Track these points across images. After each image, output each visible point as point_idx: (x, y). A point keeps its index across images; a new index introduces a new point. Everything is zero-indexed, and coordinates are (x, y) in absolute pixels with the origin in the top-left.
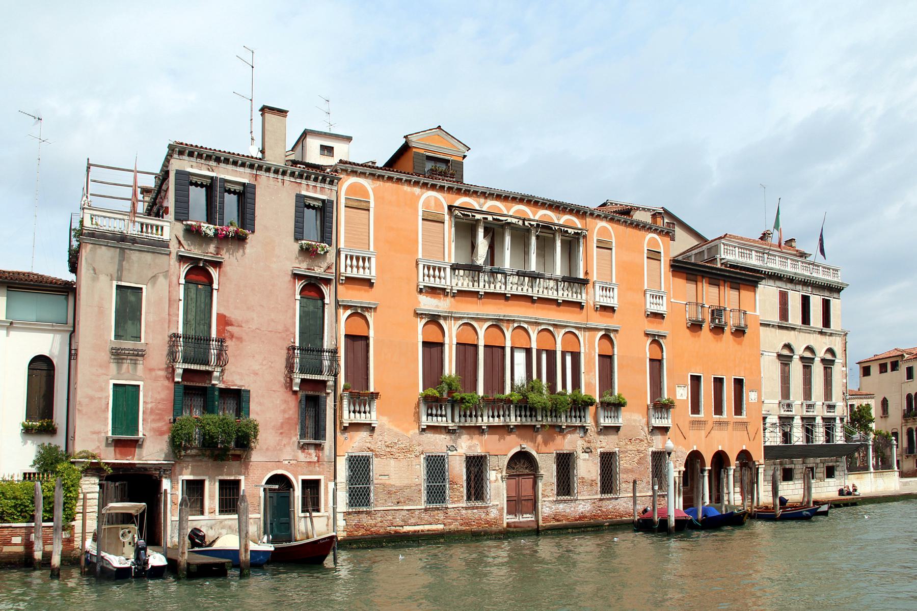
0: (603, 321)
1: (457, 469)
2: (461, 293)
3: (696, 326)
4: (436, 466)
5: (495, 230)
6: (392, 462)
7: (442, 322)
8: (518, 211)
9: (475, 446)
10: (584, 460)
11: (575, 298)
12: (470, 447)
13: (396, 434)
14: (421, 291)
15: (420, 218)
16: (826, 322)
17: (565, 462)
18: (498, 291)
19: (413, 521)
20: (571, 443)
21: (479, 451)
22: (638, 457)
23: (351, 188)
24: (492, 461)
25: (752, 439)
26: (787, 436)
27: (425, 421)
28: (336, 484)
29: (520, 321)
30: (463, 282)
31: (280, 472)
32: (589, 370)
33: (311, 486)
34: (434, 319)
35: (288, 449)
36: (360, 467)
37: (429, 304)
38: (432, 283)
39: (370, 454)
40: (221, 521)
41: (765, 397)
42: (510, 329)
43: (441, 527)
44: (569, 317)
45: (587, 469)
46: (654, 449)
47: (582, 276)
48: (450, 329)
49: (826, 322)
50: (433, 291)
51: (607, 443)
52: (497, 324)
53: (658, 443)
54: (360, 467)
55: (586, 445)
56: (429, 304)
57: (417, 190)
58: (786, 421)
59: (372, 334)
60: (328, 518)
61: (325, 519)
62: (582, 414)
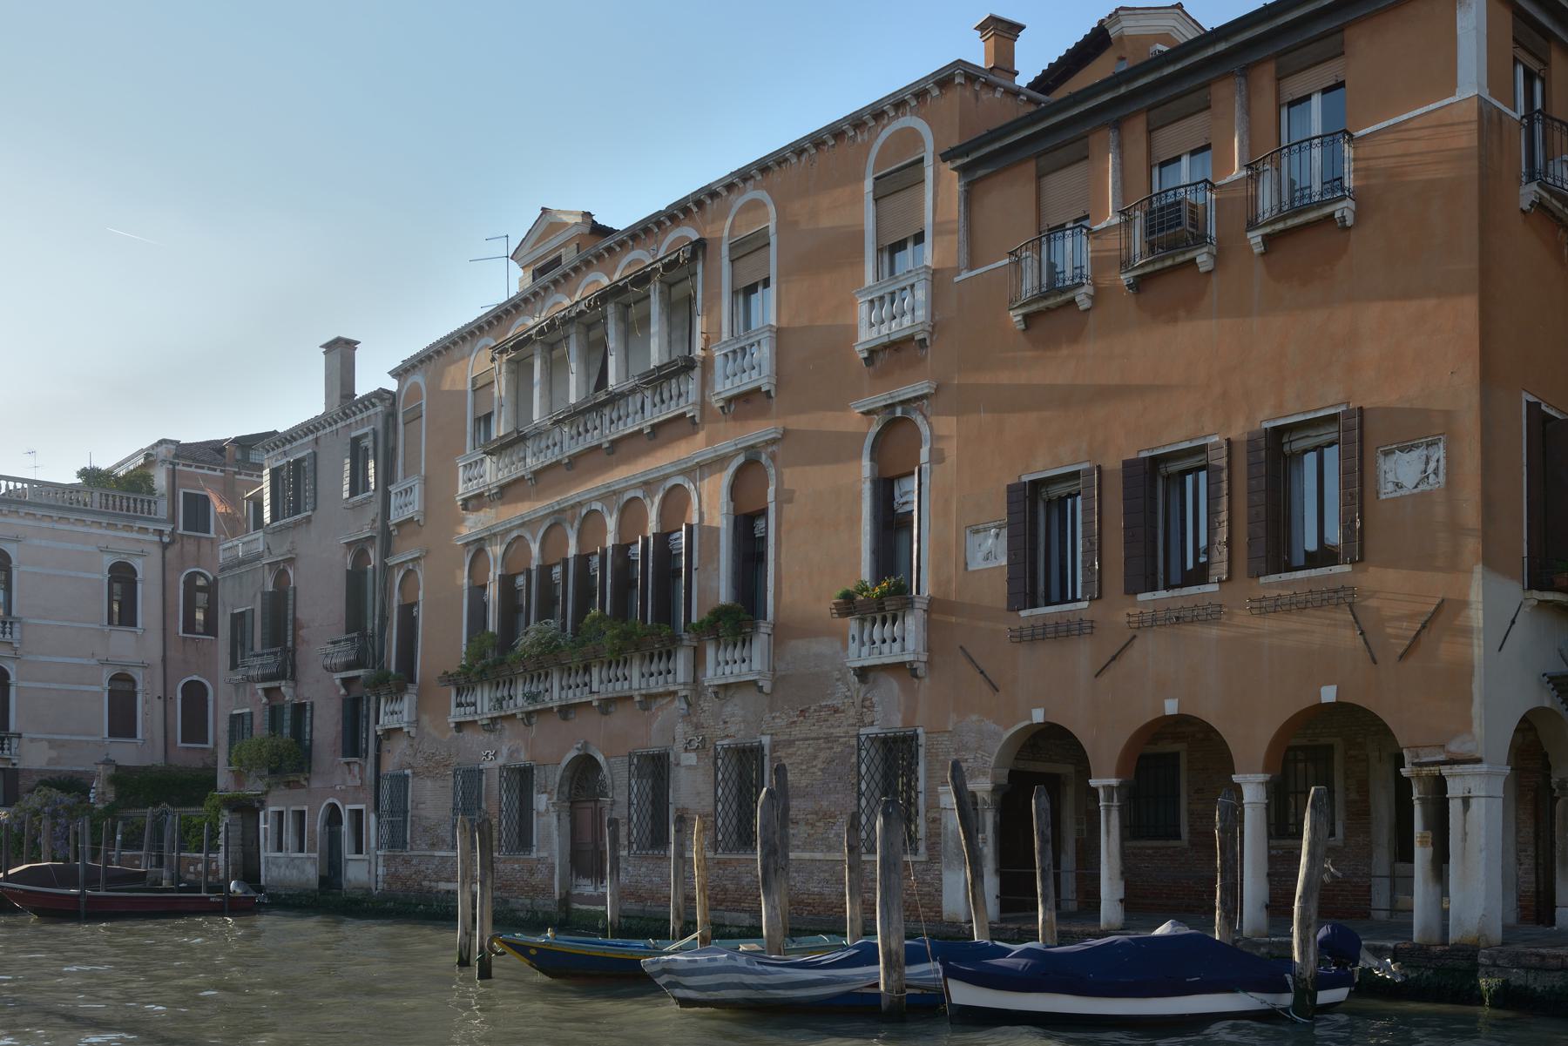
0: (734, 438)
2: (506, 492)
6: (429, 783)
10: (689, 767)
12: (511, 755)
21: (523, 758)
22: (823, 755)
27: (456, 715)
28: (378, 817)
29: (589, 501)
30: (493, 472)
31: (331, 800)
34: (478, 548)
40: (293, 859)
42: (576, 525)
50: (475, 502)
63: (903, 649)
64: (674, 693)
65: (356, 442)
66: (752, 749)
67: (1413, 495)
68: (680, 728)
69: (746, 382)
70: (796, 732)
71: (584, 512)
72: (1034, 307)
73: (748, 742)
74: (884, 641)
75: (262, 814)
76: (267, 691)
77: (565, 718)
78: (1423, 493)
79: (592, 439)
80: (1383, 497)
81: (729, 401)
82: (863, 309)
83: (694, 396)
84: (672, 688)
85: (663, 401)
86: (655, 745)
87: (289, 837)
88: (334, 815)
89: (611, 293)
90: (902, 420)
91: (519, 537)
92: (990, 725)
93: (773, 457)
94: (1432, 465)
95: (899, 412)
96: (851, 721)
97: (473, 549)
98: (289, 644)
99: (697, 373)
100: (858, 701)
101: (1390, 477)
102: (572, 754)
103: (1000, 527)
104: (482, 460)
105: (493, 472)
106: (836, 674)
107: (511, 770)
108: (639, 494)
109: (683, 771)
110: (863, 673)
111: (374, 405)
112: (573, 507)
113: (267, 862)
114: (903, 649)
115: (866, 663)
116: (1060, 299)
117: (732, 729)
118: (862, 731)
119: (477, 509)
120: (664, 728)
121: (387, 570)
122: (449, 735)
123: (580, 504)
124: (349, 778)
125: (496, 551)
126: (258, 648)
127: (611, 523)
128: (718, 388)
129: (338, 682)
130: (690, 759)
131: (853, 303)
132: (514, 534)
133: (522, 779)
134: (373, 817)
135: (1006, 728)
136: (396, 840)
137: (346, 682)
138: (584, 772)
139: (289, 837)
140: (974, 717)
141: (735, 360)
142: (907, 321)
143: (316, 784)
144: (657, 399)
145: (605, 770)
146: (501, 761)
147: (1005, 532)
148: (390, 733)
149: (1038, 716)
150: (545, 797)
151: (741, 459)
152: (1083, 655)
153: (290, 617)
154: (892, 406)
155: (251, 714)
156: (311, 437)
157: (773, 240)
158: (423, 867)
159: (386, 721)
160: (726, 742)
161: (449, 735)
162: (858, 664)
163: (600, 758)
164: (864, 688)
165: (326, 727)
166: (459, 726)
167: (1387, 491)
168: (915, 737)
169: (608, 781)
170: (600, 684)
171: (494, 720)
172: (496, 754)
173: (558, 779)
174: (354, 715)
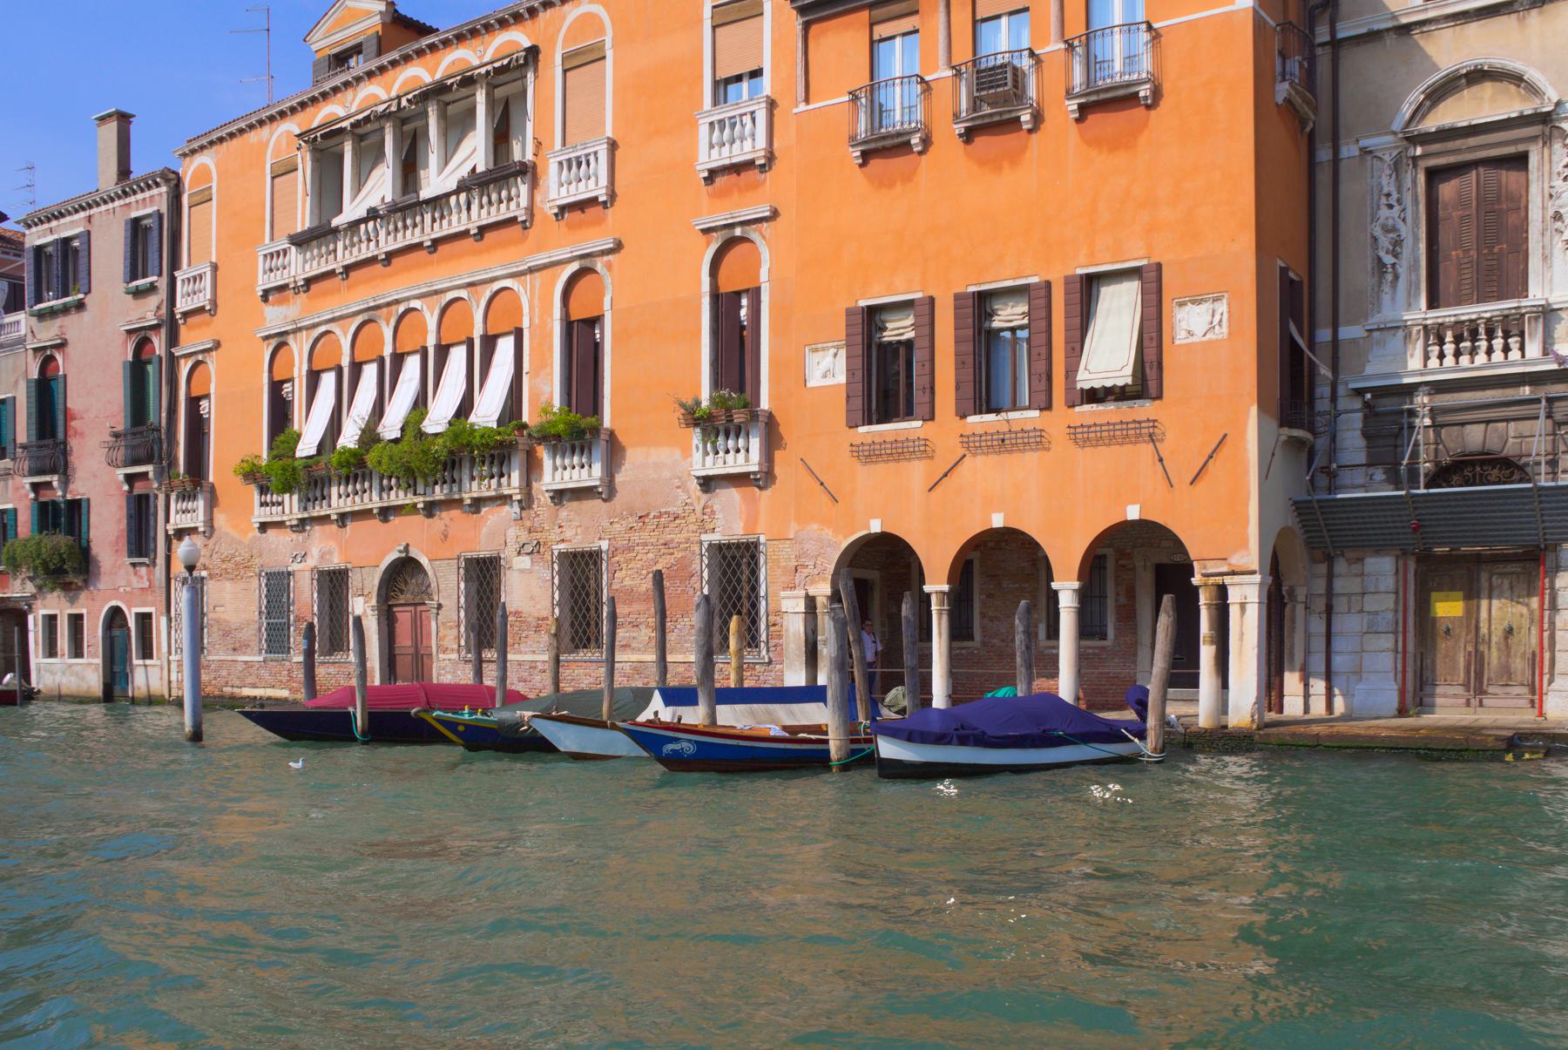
6: (228, 585)
9: (330, 552)
10: (522, 571)
11: (503, 213)
12: (322, 557)
17: (484, 575)
19: (249, 681)
20: (495, 531)
21: (336, 562)
23: (197, 177)
24: (355, 580)
25: (1183, 469)
27: (261, 514)
28: (169, 620)
29: (408, 299)
30: (299, 266)
31: (114, 603)
32: (542, 364)
34: (280, 342)
35: (122, 571)
37: (276, 317)
38: (277, 280)
40: (70, 666)
42: (393, 322)
43: (284, 693)
44: (492, 264)
45: (529, 591)
46: (716, 537)
47: (529, 157)
51: (577, 530)
53: (731, 518)
55: (524, 537)
56: (276, 317)
59: (212, 391)
62: (505, 470)
63: (747, 460)
64: (510, 496)
65: (136, 222)
66: (591, 554)
67: (1202, 343)
68: (512, 533)
69: (582, 192)
70: (635, 537)
71: (401, 308)
72: (873, 146)
73: (586, 546)
74: (727, 452)
75: (31, 618)
76: (36, 487)
77: (385, 520)
78: (1210, 342)
79: (413, 237)
80: (1177, 342)
81: (563, 209)
82: (704, 130)
83: (524, 201)
84: (506, 492)
85: (490, 203)
87: (63, 641)
88: (116, 615)
89: (438, 91)
90: (743, 239)
91: (327, 332)
92: (828, 533)
93: (609, 266)
94: (1217, 318)
95: (738, 232)
96: (692, 527)
97: (274, 342)
98: (60, 435)
99: (529, 175)
100: (699, 509)
101: (1184, 325)
103: (838, 348)
104: (285, 251)
105: (299, 266)
106: (677, 482)
107: (321, 573)
108: (463, 293)
109: (516, 574)
110: (708, 483)
111: (157, 185)
112: (389, 304)
113: (39, 671)
114: (747, 460)
115: (711, 473)
116: (900, 140)
117: (568, 534)
118: (704, 537)
119: (280, 303)
120: (495, 531)
121: (173, 361)
122: (250, 535)
123: (397, 302)
124: (134, 580)
125: (299, 348)
126: (22, 438)
127: (432, 322)
128: (553, 195)
129: (121, 478)
130: (524, 562)
131: (694, 125)
132: (322, 329)
134: (164, 620)
135: (846, 537)
137: (130, 479)
139: (63, 641)
140: (815, 527)
141: (570, 169)
142: (748, 145)
144: (485, 199)
145: (430, 573)
146: (312, 562)
147: (843, 353)
148: (181, 533)
149: (876, 527)
150: (361, 599)
151: (574, 267)
152: (917, 472)
153: (60, 407)
154: (731, 226)
155: (15, 510)
156: (82, 214)
157: (609, 54)
158: (224, 673)
159: (178, 521)
160: (562, 547)
161: (250, 535)
162: (703, 473)
163: (424, 561)
164: (705, 497)
165: (106, 527)
166: (264, 527)
167: (1181, 338)
168: (756, 545)
169: (434, 585)
171: (303, 522)
173: (376, 582)
174: (140, 514)
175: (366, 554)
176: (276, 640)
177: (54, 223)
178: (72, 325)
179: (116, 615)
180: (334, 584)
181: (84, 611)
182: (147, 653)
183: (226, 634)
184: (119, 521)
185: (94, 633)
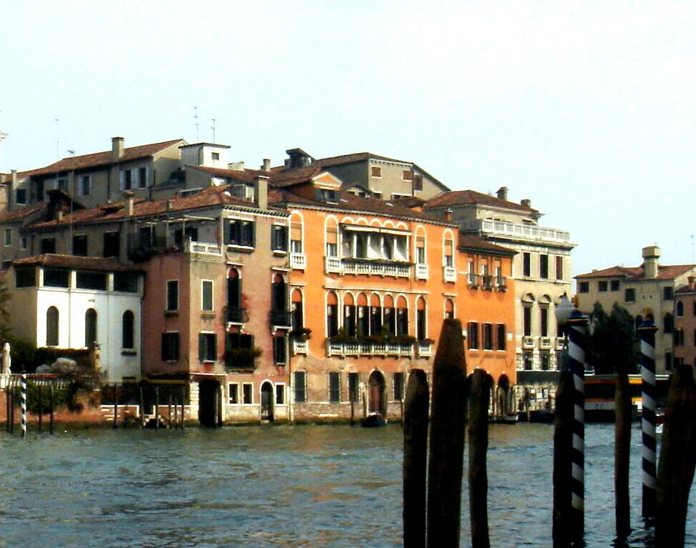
1: (345, 382)
3: (475, 288)
4: (334, 377)
5: (362, 237)
6: (314, 376)
7: (336, 292)
8: (374, 223)
13: (317, 360)
14: (326, 275)
15: (325, 231)
16: (559, 276)
18: (365, 273)
26: (528, 364)
31: (267, 380)
33: (280, 389)
34: (333, 292)
36: (300, 377)
37: (330, 283)
39: (304, 370)
40: (245, 407)
41: (515, 337)
48: (340, 294)
49: (559, 276)
50: (335, 275)
52: (364, 294)
54: (300, 377)
56: (330, 283)
57: (324, 214)
58: (528, 354)
60: (287, 407)
61: (285, 408)
86: (399, 370)
88: (267, 387)
102: (373, 370)
105: (342, 268)
113: (226, 409)
133: (354, 378)
136: (300, 396)
138: (377, 378)
143: (257, 372)
163: (383, 372)
170: (387, 350)
172: (348, 367)
175: (367, 369)
176: (335, 396)
177: (238, 212)
178: (247, 261)
179: (267, 387)
180: (354, 378)
181: (252, 383)
182: (280, 401)
183: (314, 394)
184: (269, 347)
185: (256, 392)
